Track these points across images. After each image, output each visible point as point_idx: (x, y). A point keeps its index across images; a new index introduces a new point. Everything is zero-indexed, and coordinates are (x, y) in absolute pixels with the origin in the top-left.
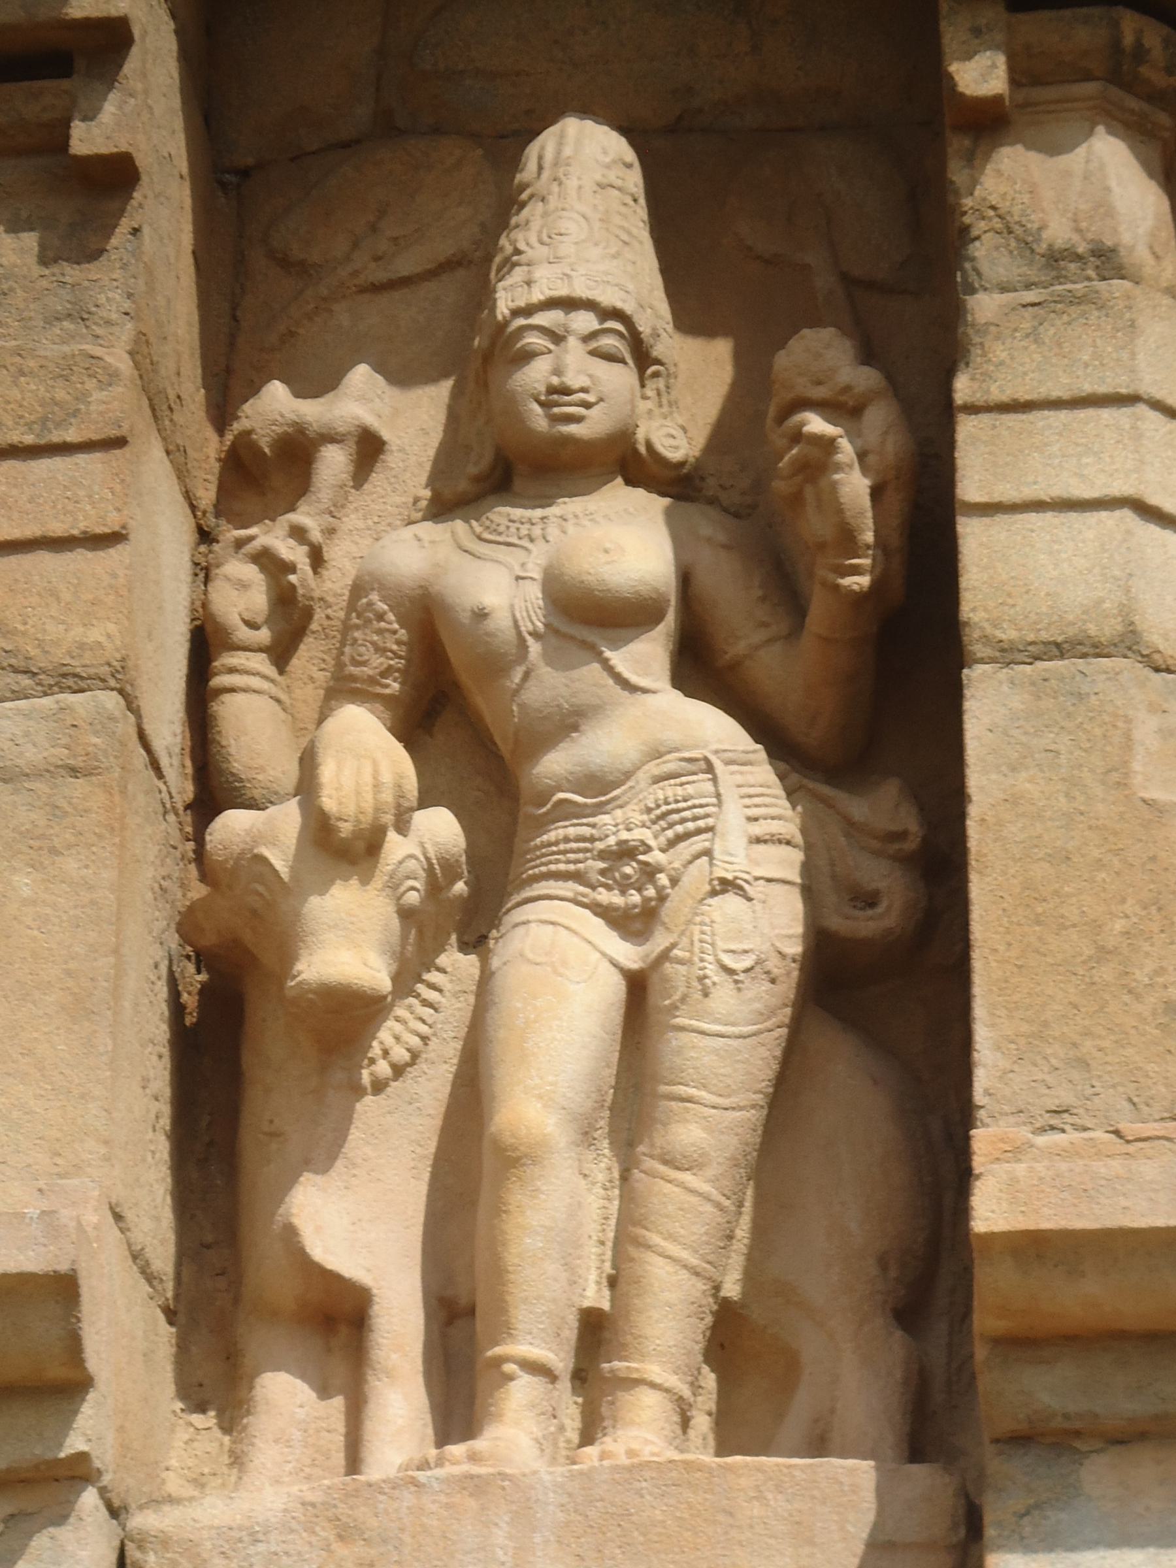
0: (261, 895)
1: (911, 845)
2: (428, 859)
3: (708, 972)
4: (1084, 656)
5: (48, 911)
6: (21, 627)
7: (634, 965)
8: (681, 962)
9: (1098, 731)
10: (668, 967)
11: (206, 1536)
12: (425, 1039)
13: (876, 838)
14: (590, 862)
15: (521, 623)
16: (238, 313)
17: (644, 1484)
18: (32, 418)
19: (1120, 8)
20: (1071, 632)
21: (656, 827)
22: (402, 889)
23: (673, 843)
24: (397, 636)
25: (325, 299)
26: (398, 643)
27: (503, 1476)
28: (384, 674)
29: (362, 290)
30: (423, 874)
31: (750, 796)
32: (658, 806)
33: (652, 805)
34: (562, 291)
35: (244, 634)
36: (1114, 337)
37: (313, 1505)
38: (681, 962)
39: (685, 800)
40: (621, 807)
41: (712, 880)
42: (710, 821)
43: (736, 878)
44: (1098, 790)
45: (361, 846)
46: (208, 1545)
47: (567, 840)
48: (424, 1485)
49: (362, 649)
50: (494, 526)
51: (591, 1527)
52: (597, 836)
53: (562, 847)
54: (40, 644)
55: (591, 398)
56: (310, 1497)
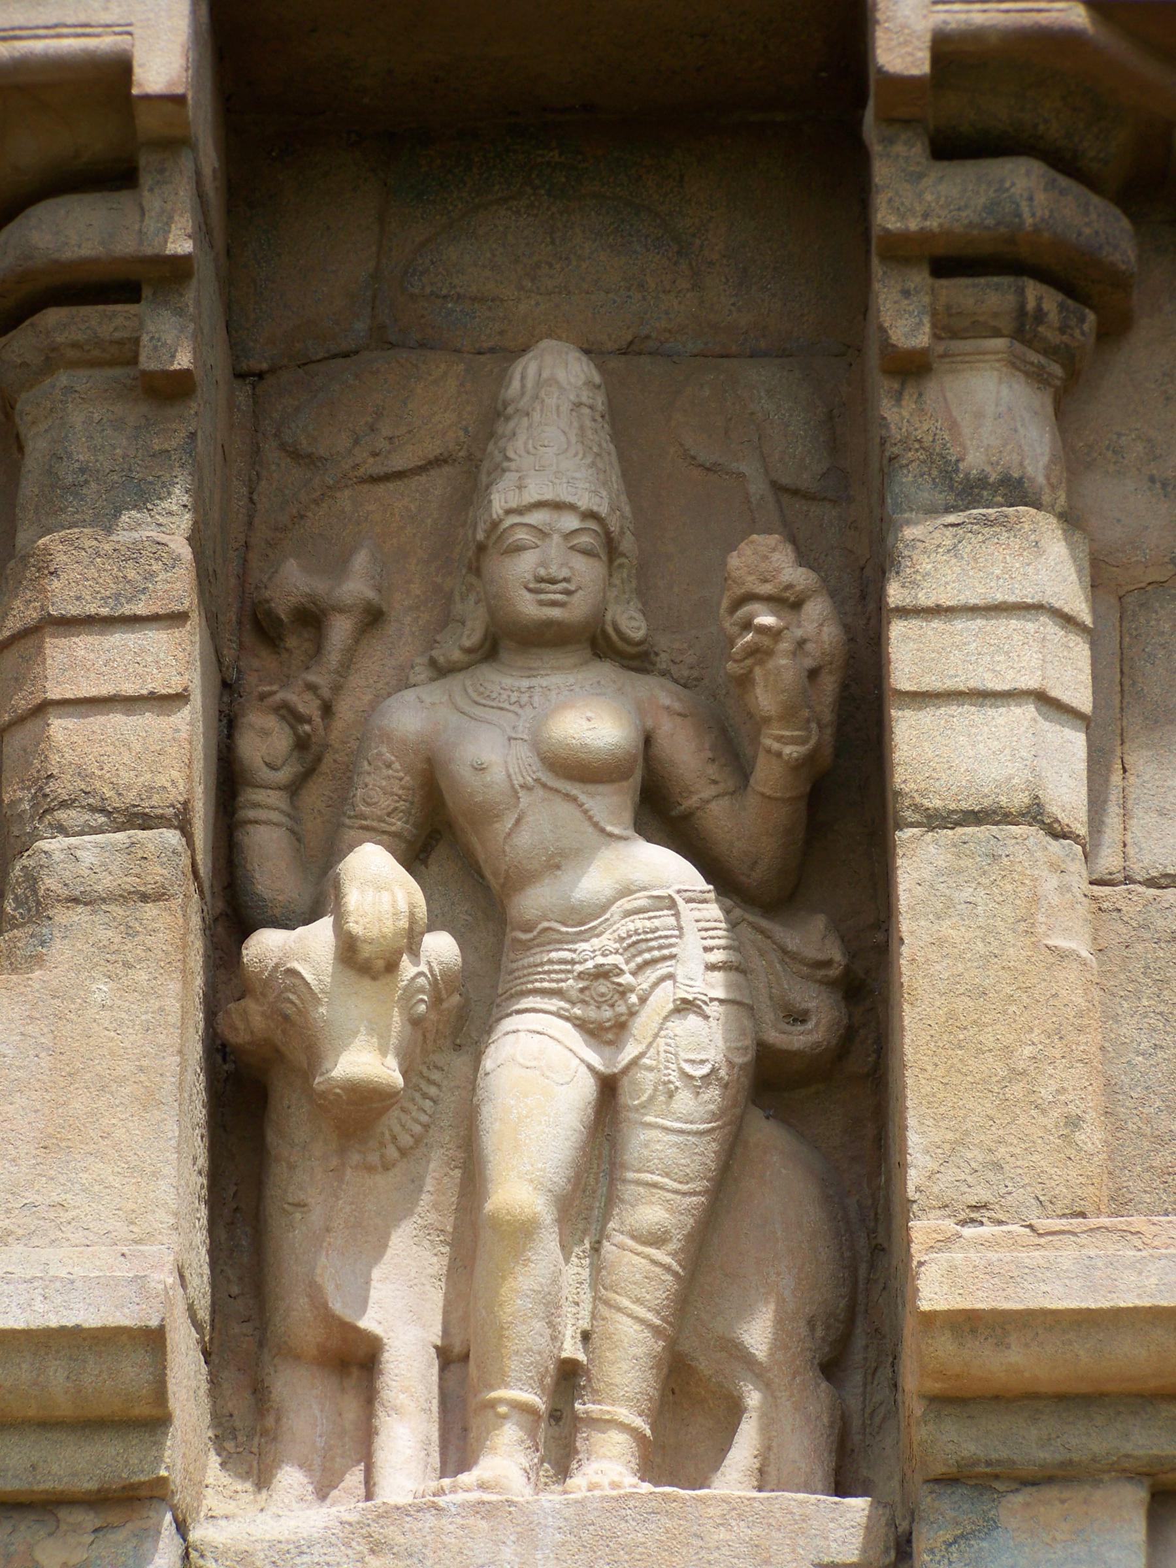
0: (292, 1002)
1: (834, 972)
3: (671, 1078)
4: (997, 823)
5: (123, 1015)
8: (650, 1069)
9: (1009, 887)
11: (260, 1548)
12: (426, 1127)
13: (805, 965)
14: (571, 982)
15: (514, 777)
16: (255, 497)
17: (629, 1512)
19: (1025, 279)
20: (986, 803)
23: (641, 968)
24: (403, 783)
26: (403, 788)
27: (510, 1503)
28: (389, 815)
29: (362, 481)
31: (706, 930)
32: (630, 936)
34: (548, 496)
35: (266, 774)
36: (1021, 555)
37: (350, 1524)
38: (650, 1069)
39: (653, 932)
40: (598, 936)
41: (675, 1000)
42: (674, 950)
43: (695, 999)
44: (1010, 937)
45: (380, 964)
48: (443, 1509)
49: (372, 793)
50: (488, 693)
51: (584, 1546)
52: (577, 960)
53: (546, 968)
55: (572, 587)
56: (347, 1517)
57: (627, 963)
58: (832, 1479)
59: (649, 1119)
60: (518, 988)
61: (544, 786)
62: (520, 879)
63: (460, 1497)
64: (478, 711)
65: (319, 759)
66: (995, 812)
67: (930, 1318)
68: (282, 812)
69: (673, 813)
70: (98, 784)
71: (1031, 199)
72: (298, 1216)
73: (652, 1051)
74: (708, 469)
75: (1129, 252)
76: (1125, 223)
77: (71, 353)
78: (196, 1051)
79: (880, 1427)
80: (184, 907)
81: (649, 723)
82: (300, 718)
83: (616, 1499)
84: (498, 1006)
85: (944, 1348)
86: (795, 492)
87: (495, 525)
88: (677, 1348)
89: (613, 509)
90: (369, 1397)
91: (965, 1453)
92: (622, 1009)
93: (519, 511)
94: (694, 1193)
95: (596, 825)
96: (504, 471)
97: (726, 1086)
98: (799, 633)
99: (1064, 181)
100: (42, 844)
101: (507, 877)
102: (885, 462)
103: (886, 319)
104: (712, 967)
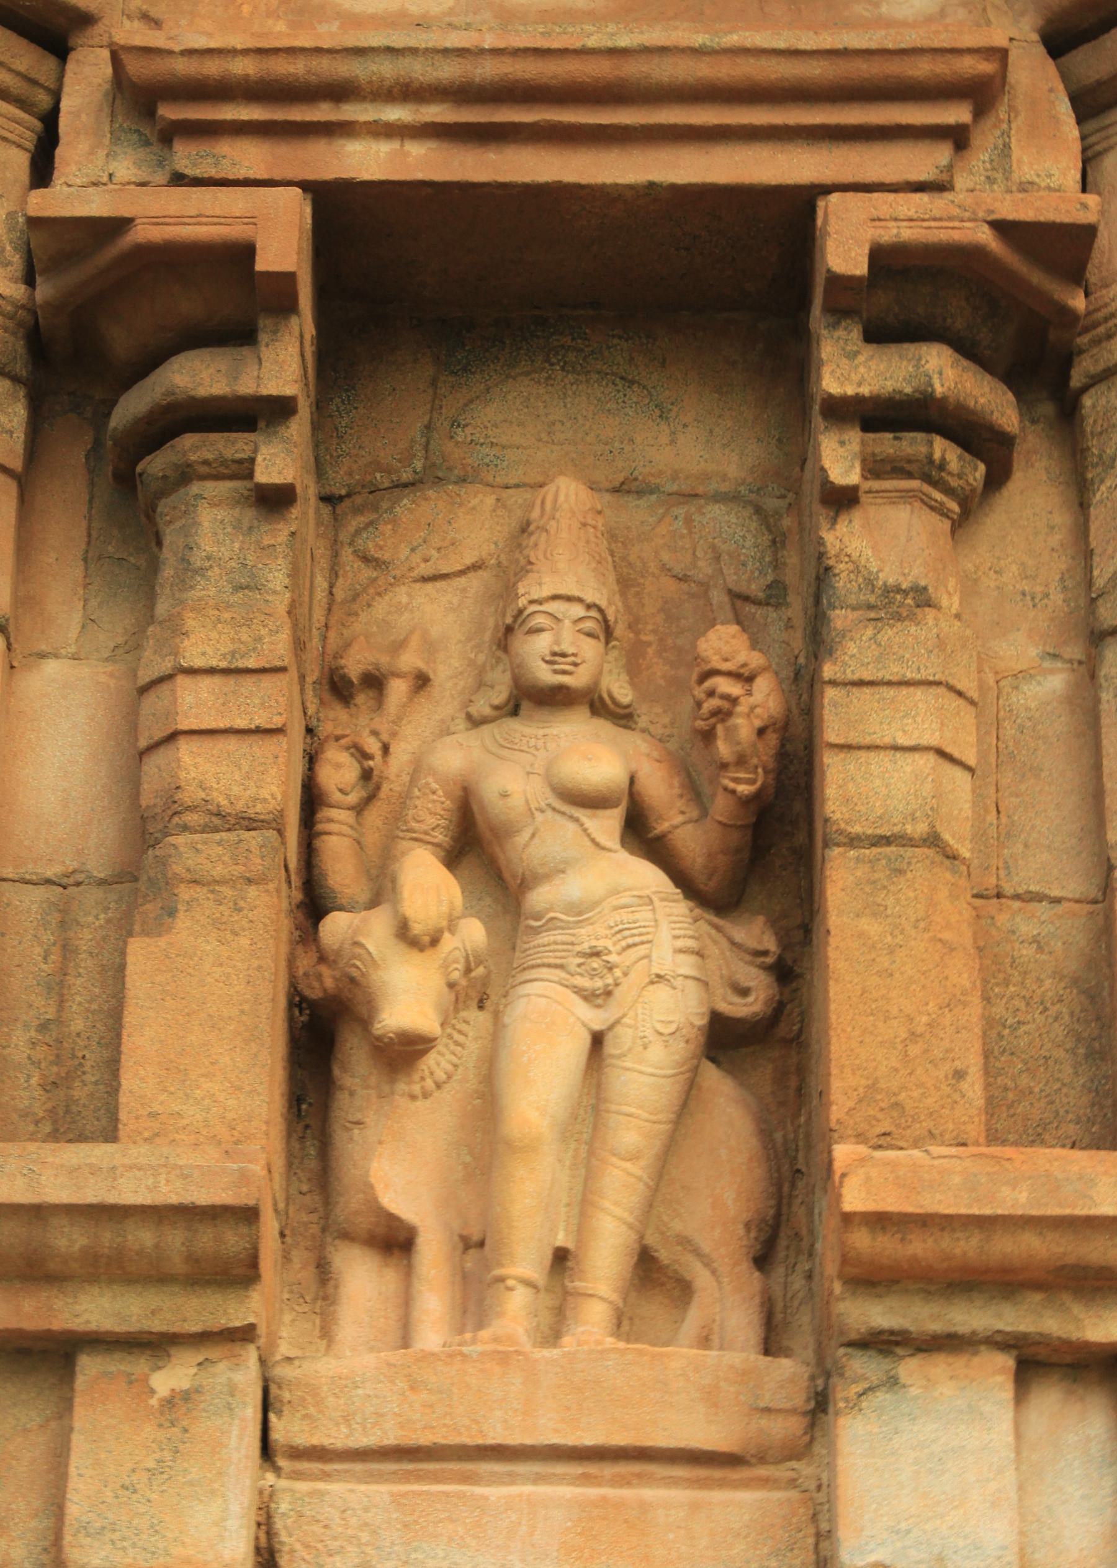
0: (357, 967)
1: (769, 960)
2: (466, 950)
3: (646, 1034)
5: (230, 970)
6: (215, 786)
7: (597, 1027)
8: (630, 1026)
9: (911, 894)
10: (618, 1029)
12: (456, 1066)
16: (334, 590)
17: (610, 1363)
18: (227, 650)
20: (896, 829)
21: (614, 939)
22: (450, 969)
23: (624, 949)
25: (391, 584)
26: (444, 810)
28: (433, 829)
29: (416, 581)
30: (462, 960)
31: (675, 922)
33: (612, 924)
35: (337, 796)
37: (395, 1366)
38: (630, 1026)
39: (635, 922)
40: (592, 924)
42: (649, 937)
44: (913, 933)
45: (427, 939)
46: (325, 1388)
47: (555, 943)
49: (421, 813)
53: (552, 948)
54: (228, 796)
55: (578, 661)
57: (615, 944)
58: (762, 1346)
59: (628, 1064)
60: (530, 963)
61: (554, 809)
62: (525, 884)
63: (479, 1348)
64: (505, 753)
65: (378, 788)
66: (901, 837)
67: (848, 1219)
68: (351, 827)
69: (650, 835)
70: (215, 794)
71: (941, 373)
72: (356, 1131)
73: (631, 1014)
74: (680, 579)
75: (1013, 417)
76: (1010, 395)
77: (203, 470)
78: (282, 1002)
79: (798, 1308)
80: (278, 891)
81: (634, 766)
82: (367, 756)
83: (601, 1352)
84: (513, 976)
85: (862, 1240)
86: (746, 599)
87: (521, 612)
88: (645, 1242)
89: (610, 603)
90: (408, 1273)
91: (873, 1324)
92: (610, 981)
93: (539, 602)
94: (660, 1123)
95: (593, 841)
96: (528, 572)
97: (687, 1042)
98: (752, 700)
99: (965, 363)
100: (171, 839)
101: (523, 880)
102: (822, 571)
103: (827, 463)
104: (681, 951)
